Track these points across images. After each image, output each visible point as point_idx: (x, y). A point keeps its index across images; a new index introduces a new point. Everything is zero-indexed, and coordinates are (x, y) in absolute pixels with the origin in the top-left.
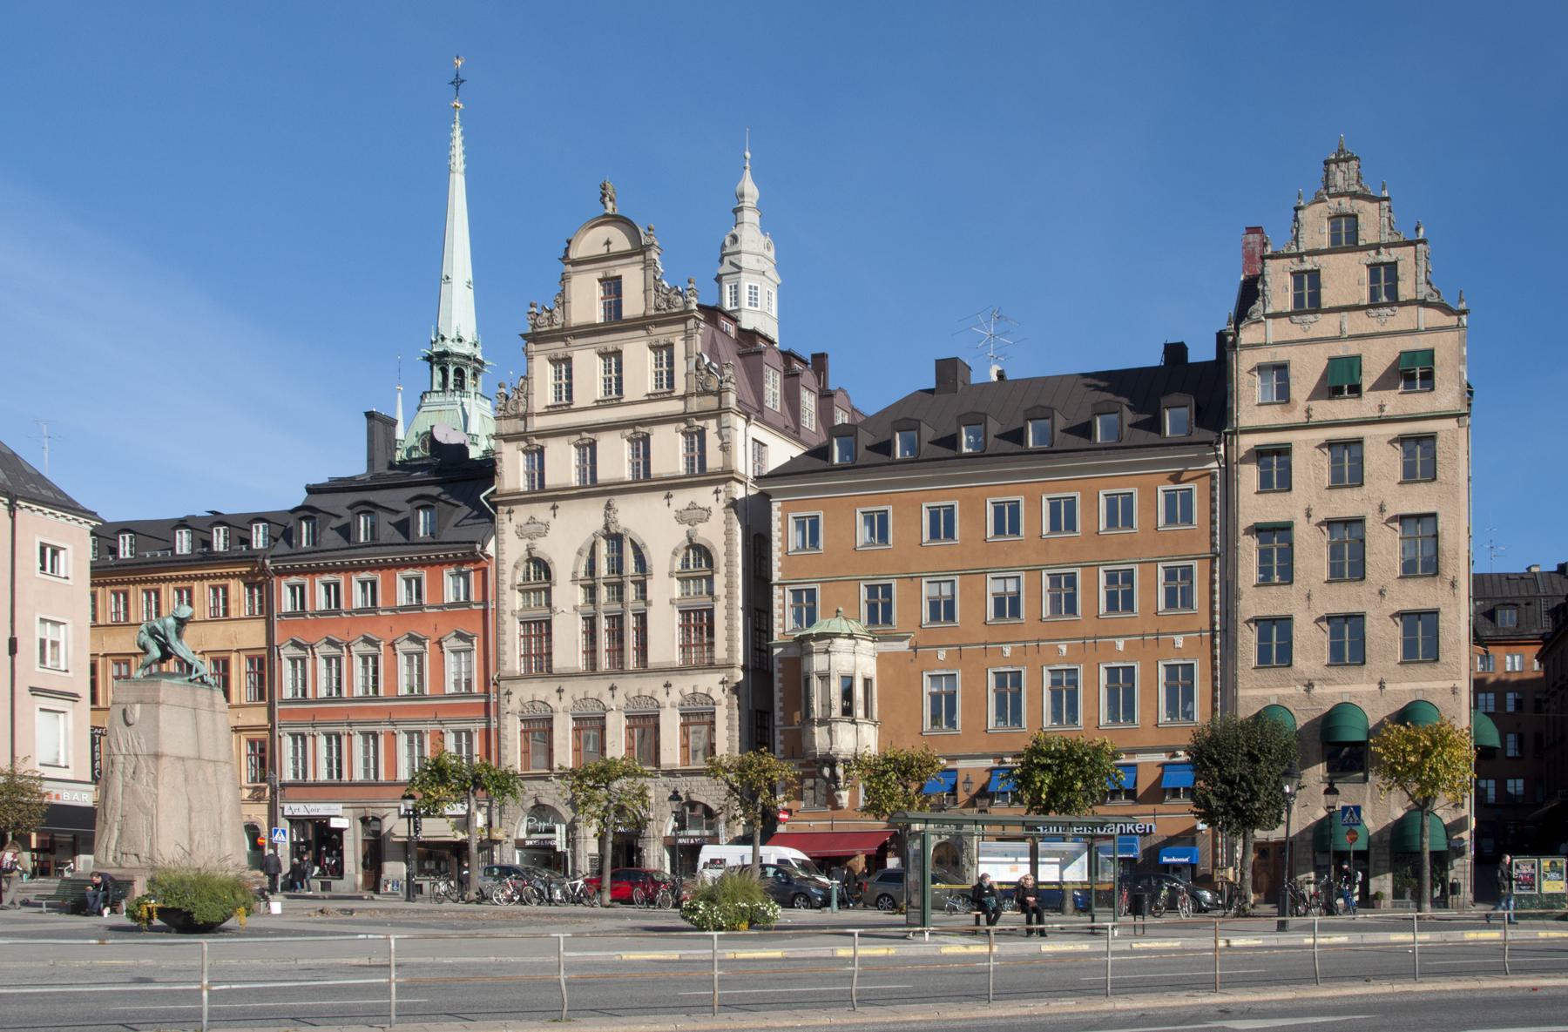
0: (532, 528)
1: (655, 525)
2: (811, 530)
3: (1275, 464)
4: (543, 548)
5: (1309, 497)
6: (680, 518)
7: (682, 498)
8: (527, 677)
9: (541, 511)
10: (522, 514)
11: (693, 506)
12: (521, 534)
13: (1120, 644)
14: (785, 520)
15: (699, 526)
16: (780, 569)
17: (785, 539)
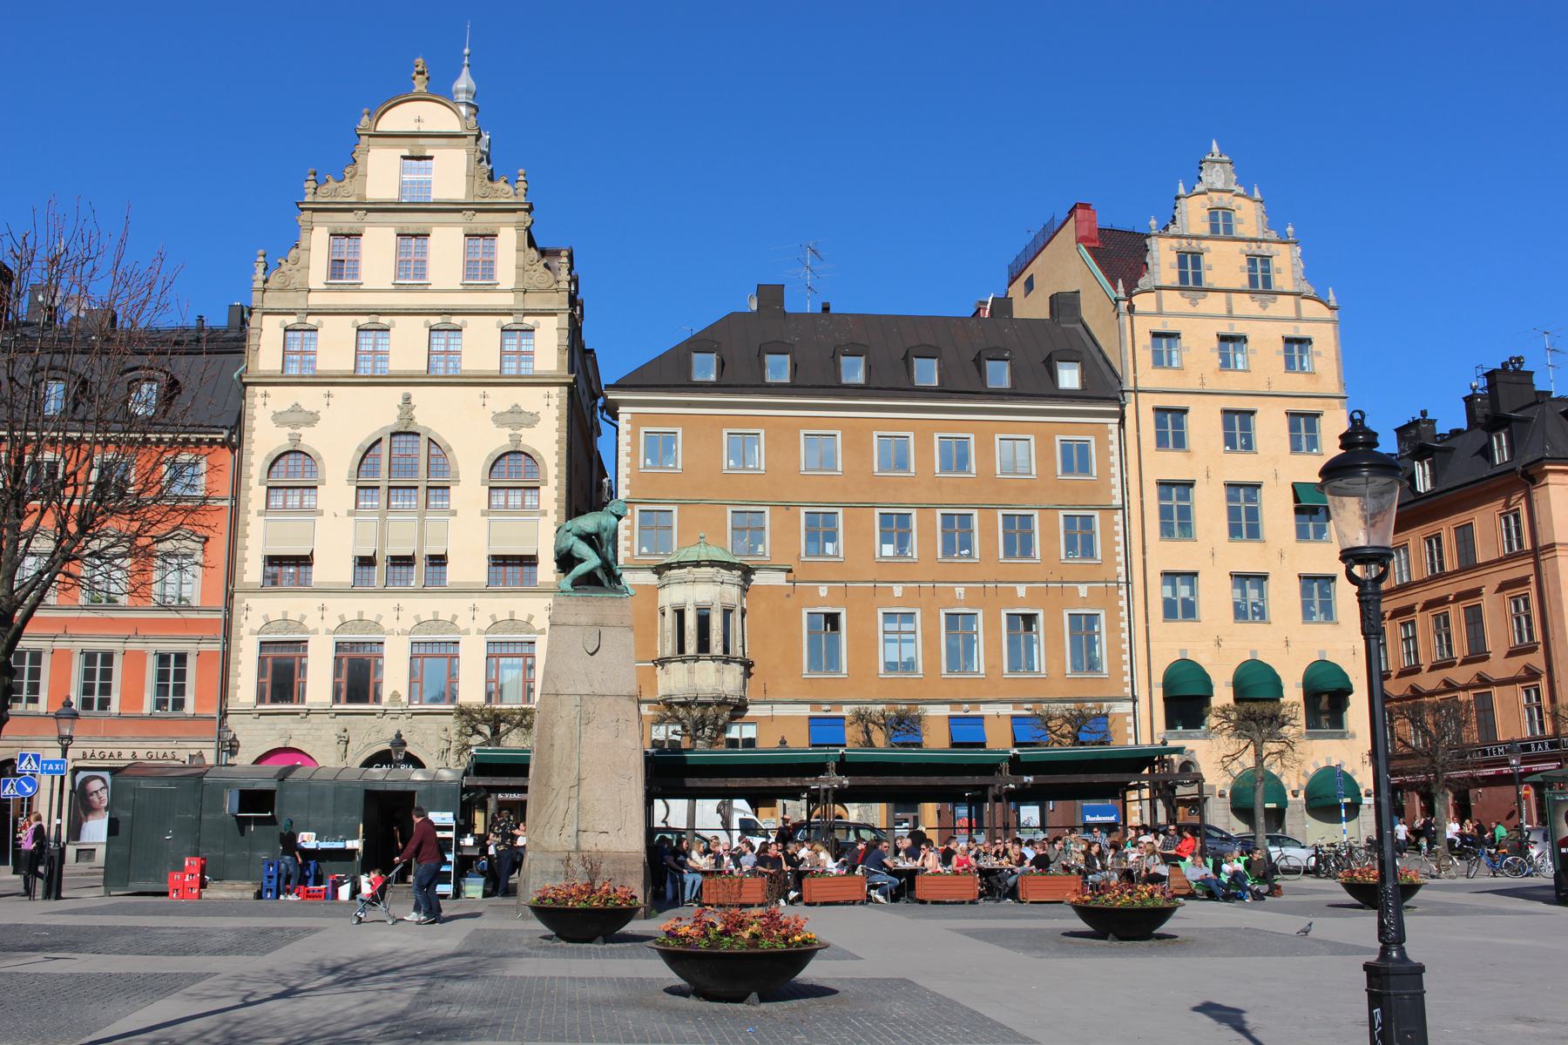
0: (294, 417)
1: (466, 427)
2: (659, 446)
3: (1171, 425)
4: (310, 439)
5: (1207, 461)
6: (499, 419)
7: (502, 398)
8: (261, 590)
9: (309, 398)
10: (282, 398)
11: (516, 411)
12: (279, 419)
13: (1021, 590)
14: (634, 434)
15: (523, 431)
16: (627, 487)
17: (633, 455)
